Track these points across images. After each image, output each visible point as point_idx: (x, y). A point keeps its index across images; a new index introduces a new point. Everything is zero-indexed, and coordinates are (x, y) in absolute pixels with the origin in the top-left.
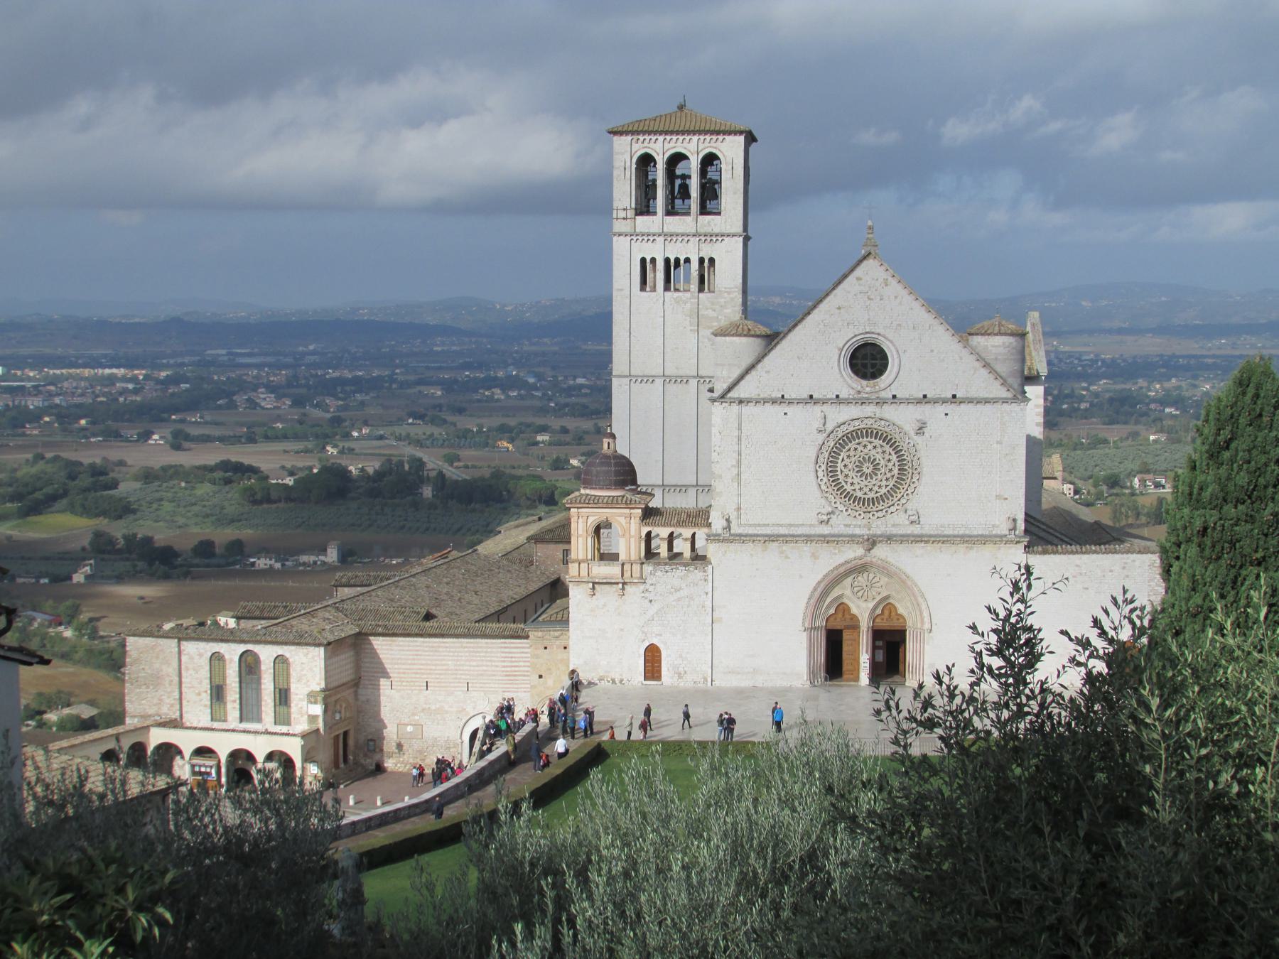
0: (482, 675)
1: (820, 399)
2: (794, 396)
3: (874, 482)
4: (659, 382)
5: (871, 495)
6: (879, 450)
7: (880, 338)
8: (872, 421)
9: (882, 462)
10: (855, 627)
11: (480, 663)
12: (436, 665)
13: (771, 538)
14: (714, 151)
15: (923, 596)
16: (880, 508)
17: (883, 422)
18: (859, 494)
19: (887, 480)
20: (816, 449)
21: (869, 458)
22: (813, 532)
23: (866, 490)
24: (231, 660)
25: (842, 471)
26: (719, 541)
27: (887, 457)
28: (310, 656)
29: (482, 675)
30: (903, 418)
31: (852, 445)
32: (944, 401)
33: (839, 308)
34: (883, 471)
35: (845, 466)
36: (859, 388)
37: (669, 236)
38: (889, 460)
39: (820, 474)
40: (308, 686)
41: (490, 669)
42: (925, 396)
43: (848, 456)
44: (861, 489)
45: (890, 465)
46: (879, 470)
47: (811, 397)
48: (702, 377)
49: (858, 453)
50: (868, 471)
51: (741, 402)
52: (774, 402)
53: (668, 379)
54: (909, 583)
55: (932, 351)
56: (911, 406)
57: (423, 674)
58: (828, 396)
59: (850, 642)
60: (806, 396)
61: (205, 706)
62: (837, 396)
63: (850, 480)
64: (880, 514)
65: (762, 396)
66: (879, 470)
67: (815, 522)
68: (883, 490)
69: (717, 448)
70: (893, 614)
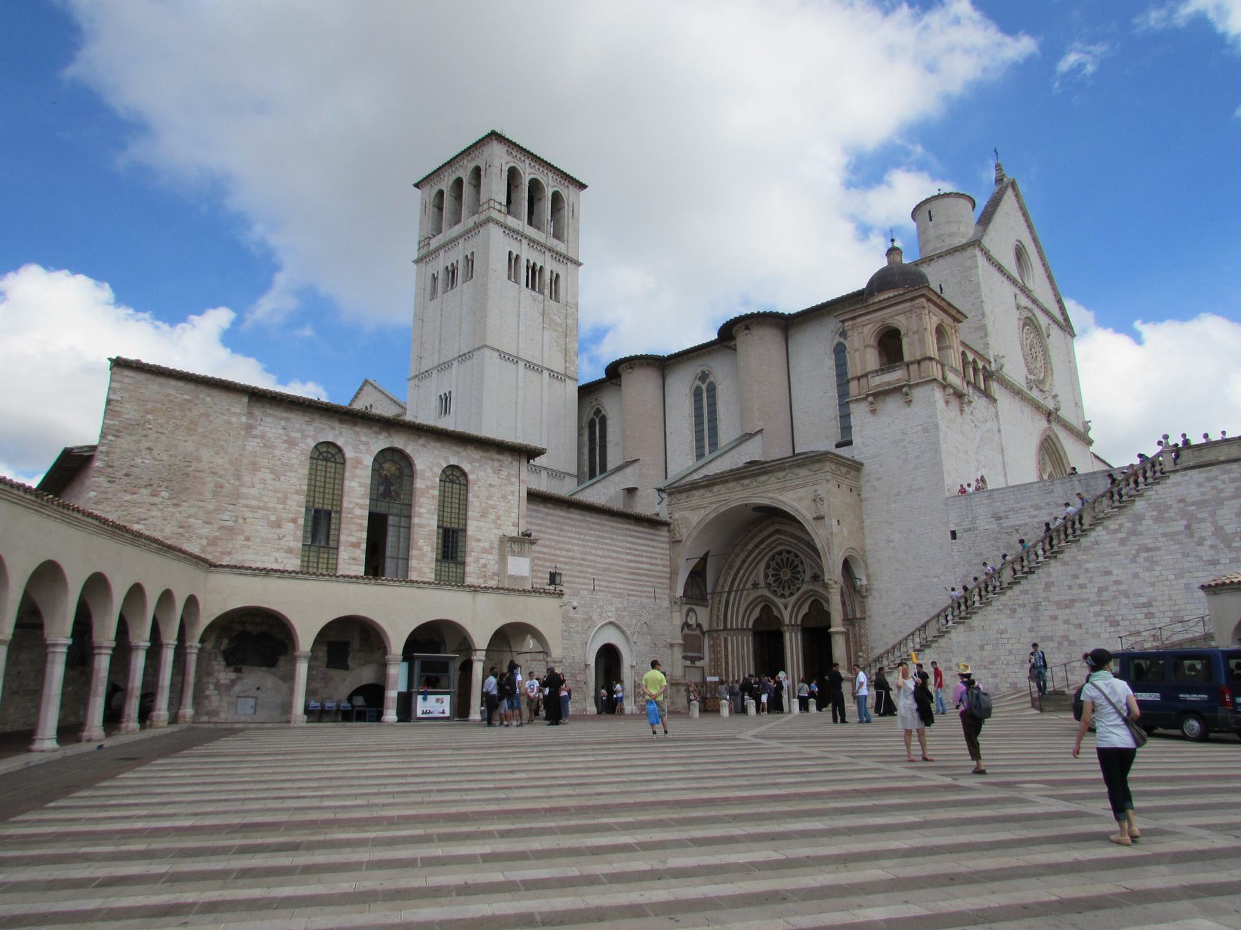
0: (608, 570)
4: (521, 364)
11: (606, 553)
12: (559, 549)
14: (561, 192)
24: (358, 462)
28: (504, 473)
29: (608, 570)
37: (532, 242)
40: (499, 527)
41: (615, 562)
48: (552, 371)
53: (530, 366)
57: (545, 560)
61: (290, 551)
68: (1042, 376)
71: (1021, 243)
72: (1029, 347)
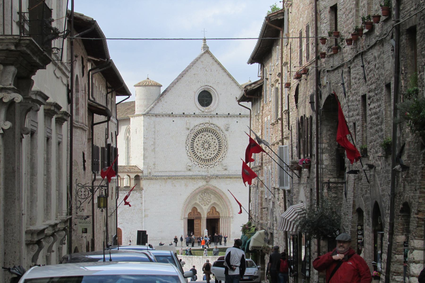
1: (187, 115)
2: (177, 113)
3: (209, 152)
5: (208, 158)
6: (211, 138)
7: (211, 88)
9: (212, 143)
10: (200, 218)
13: (170, 178)
15: (230, 202)
16: (211, 163)
17: (212, 125)
18: (203, 157)
19: (214, 151)
20: (186, 137)
21: (207, 141)
22: (185, 174)
23: (206, 155)
25: (196, 147)
26: (147, 179)
27: (214, 141)
30: (220, 123)
31: (200, 135)
32: (237, 116)
33: (194, 75)
34: (212, 147)
35: (197, 145)
36: (203, 110)
38: (215, 142)
39: (188, 148)
42: (229, 114)
43: (199, 141)
45: (215, 144)
46: (211, 146)
47: (184, 113)
49: (202, 139)
50: (206, 147)
51: (156, 116)
52: (169, 116)
54: (224, 197)
55: (231, 94)
56: (223, 118)
58: (191, 113)
59: (197, 225)
60: (182, 113)
62: (194, 114)
63: (199, 151)
65: (164, 113)
66: (211, 146)
67: (185, 170)
68: (213, 156)
69: (145, 137)
70: (214, 211)
71: (208, 86)
72: (200, 145)
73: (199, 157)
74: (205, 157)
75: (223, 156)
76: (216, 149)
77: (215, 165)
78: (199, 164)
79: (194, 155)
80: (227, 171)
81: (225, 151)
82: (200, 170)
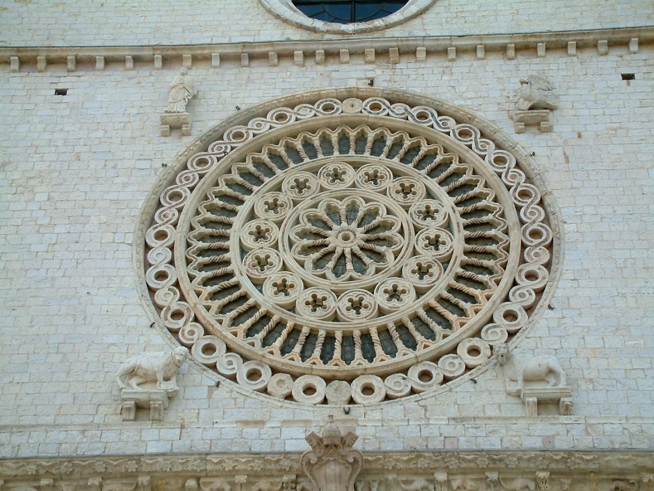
3: (368, 279)
8: (359, 105)
9: (402, 218)
17: (399, 108)
19: (422, 271)
27: (419, 203)
35: (260, 234)
38: (428, 214)
39: (159, 256)
43: (273, 206)
44: (316, 303)
45: (432, 228)
46: (388, 242)
56: (495, 62)
63: (273, 275)
64: (395, 384)
66: (388, 242)
68: (409, 305)
73: (266, 317)
74: (336, 318)
75: (515, 306)
76: (446, 262)
77: (437, 377)
78: (266, 373)
79: (216, 304)
80: (563, 419)
81: (533, 266)
82: (259, 418)
